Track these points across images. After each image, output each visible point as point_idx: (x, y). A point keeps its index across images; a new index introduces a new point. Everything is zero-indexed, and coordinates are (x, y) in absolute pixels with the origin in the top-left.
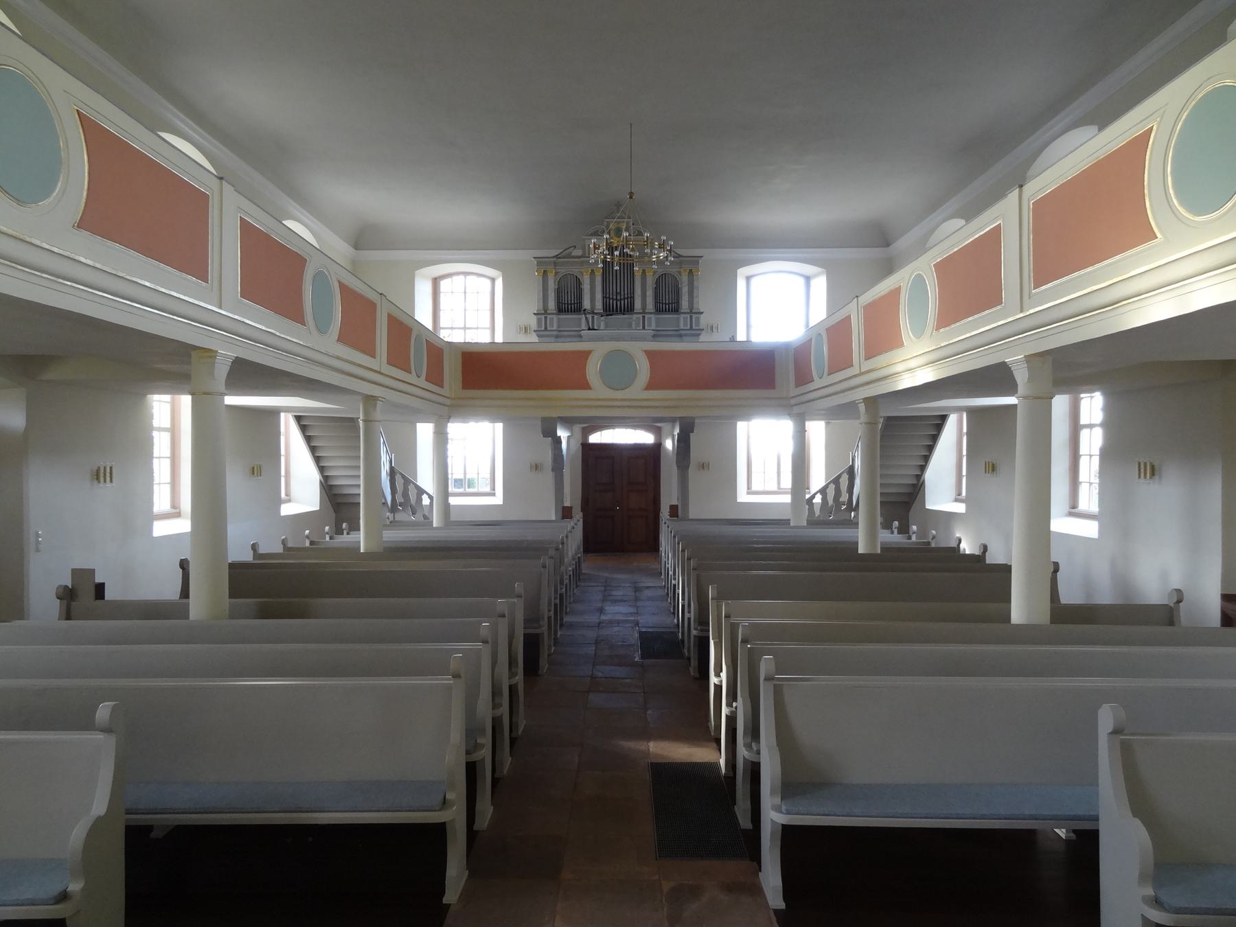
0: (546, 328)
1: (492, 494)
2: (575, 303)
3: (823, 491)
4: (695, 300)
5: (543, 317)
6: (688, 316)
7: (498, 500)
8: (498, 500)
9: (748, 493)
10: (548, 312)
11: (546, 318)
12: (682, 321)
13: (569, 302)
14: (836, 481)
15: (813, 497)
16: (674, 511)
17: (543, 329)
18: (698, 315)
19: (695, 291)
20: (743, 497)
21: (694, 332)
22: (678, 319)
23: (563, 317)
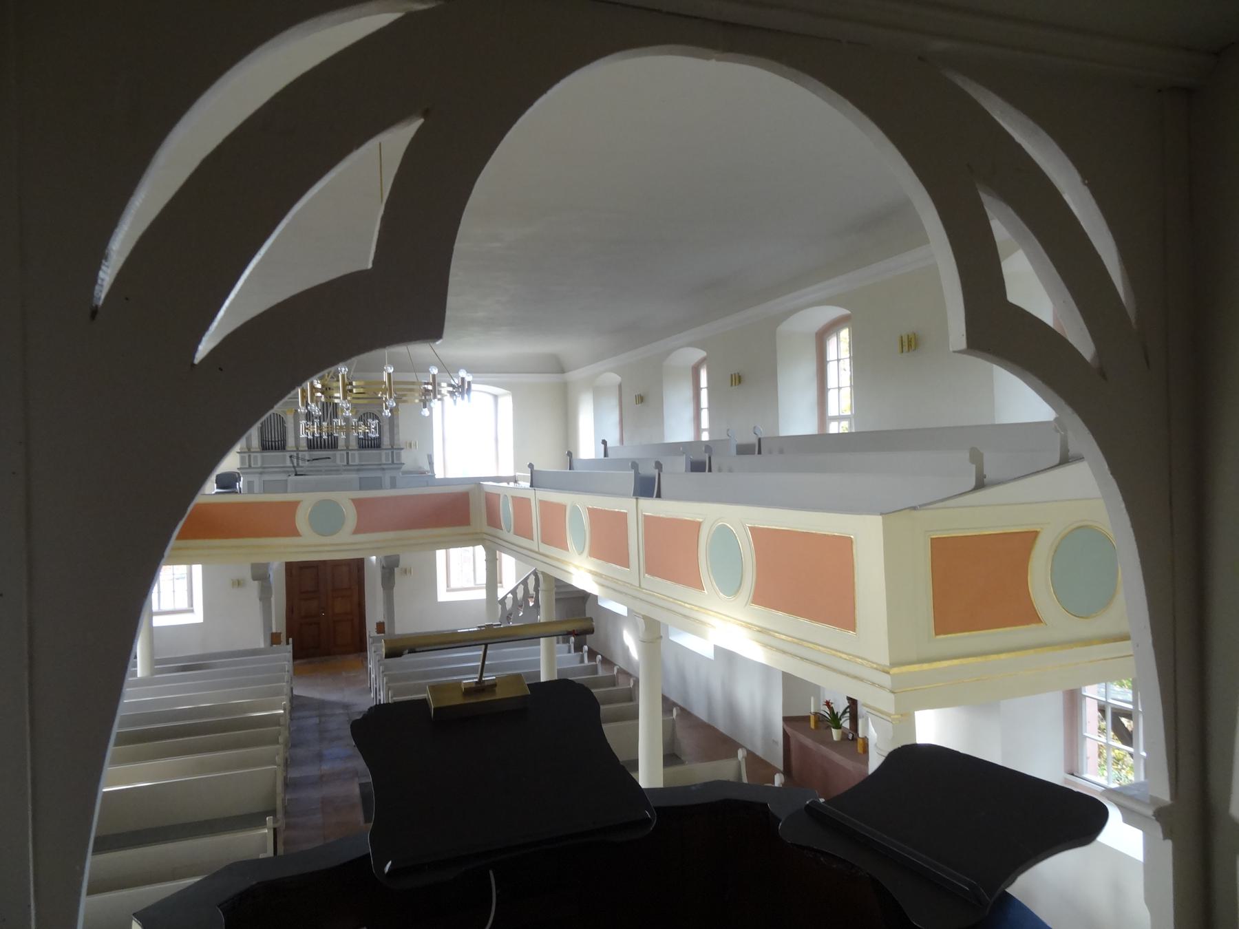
0: (250, 466)
1: (190, 610)
2: (279, 441)
3: (514, 592)
4: (396, 438)
5: (246, 455)
6: (390, 452)
7: (197, 617)
8: (197, 617)
9: (447, 591)
10: (252, 450)
11: (249, 456)
12: (384, 456)
13: (273, 440)
14: (525, 582)
15: (505, 597)
16: (380, 627)
17: (247, 466)
18: (398, 451)
19: (395, 429)
20: (443, 596)
21: (395, 466)
22: (380, 454)
23: (269, 454)
